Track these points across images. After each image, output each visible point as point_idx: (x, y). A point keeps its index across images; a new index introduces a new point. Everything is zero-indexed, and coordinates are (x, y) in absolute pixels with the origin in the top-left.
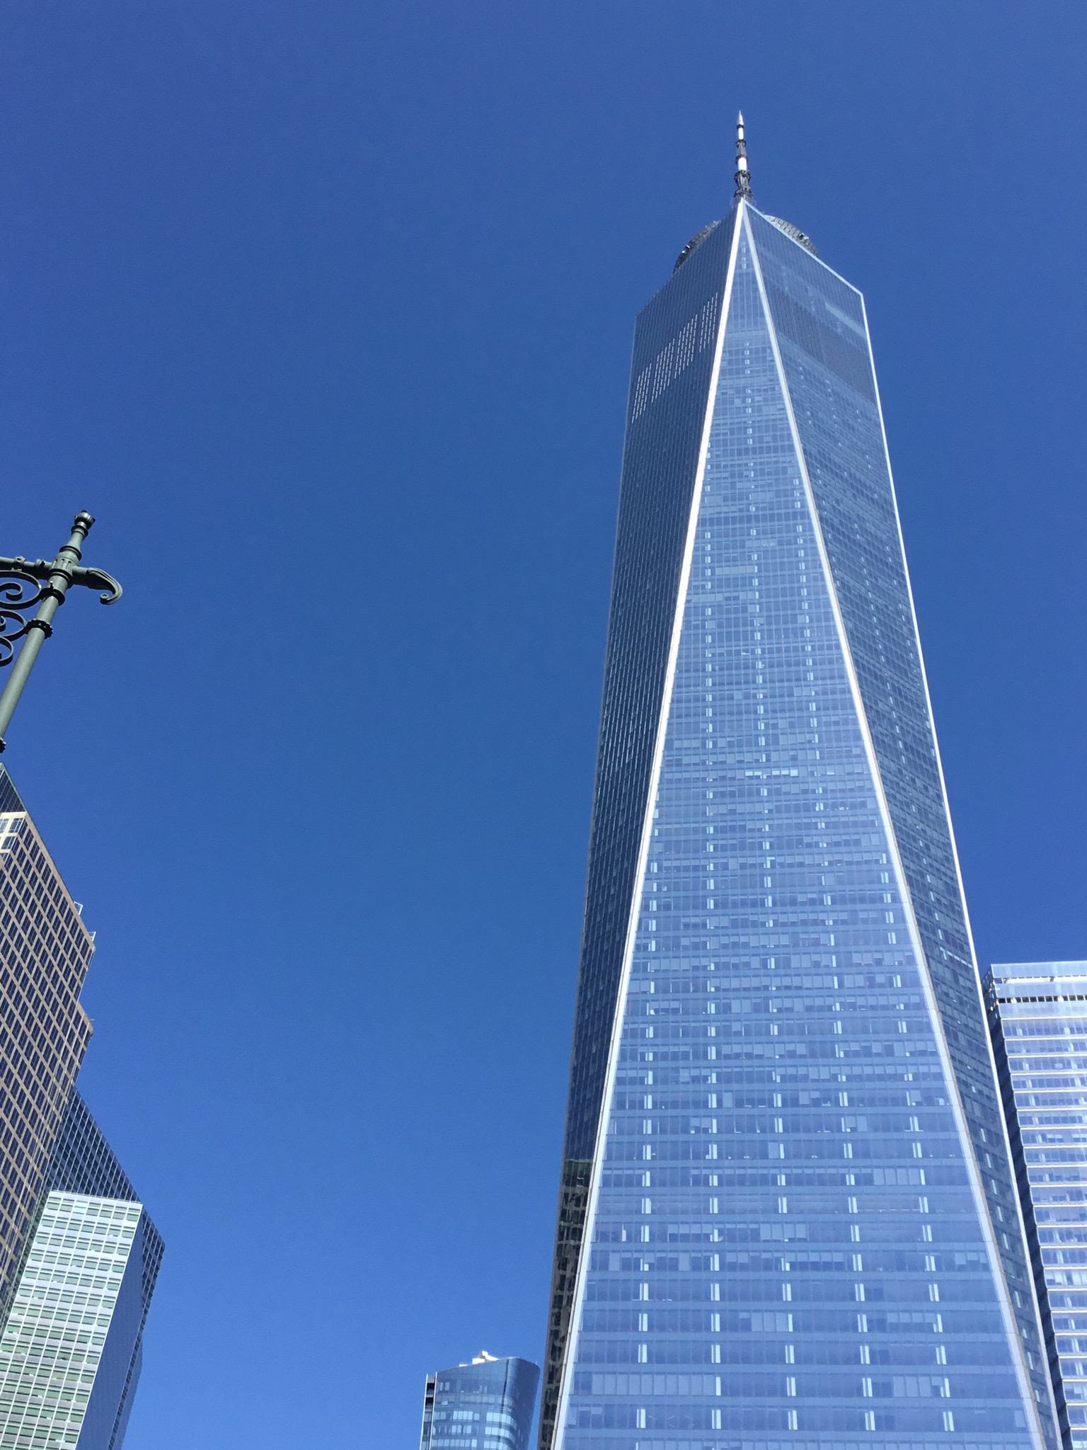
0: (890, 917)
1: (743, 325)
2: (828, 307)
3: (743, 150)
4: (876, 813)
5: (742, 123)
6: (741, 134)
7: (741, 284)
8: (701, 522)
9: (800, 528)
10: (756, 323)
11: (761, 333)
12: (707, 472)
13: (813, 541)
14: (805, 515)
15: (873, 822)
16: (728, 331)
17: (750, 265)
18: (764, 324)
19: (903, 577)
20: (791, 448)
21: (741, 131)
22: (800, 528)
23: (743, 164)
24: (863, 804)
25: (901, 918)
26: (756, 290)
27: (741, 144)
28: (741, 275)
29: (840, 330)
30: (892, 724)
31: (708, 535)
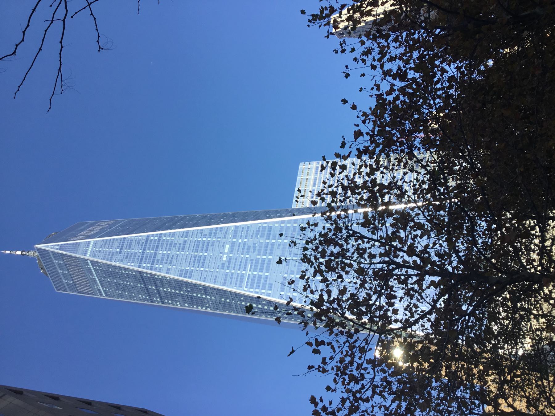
0: (277, 225)
2: (80, 229)
3: (12, 252)
6: (8, 252)
8: (139, 266)
9: (152, 238)
13: (157, 234)
14: (148, 236)
18: (80, 243)
20: (124, 238)
22: (152, 238)
23: (19, 253)
25: (277, 222)
26: (67, 244)
27: (12, 252)
31: (144, 265)
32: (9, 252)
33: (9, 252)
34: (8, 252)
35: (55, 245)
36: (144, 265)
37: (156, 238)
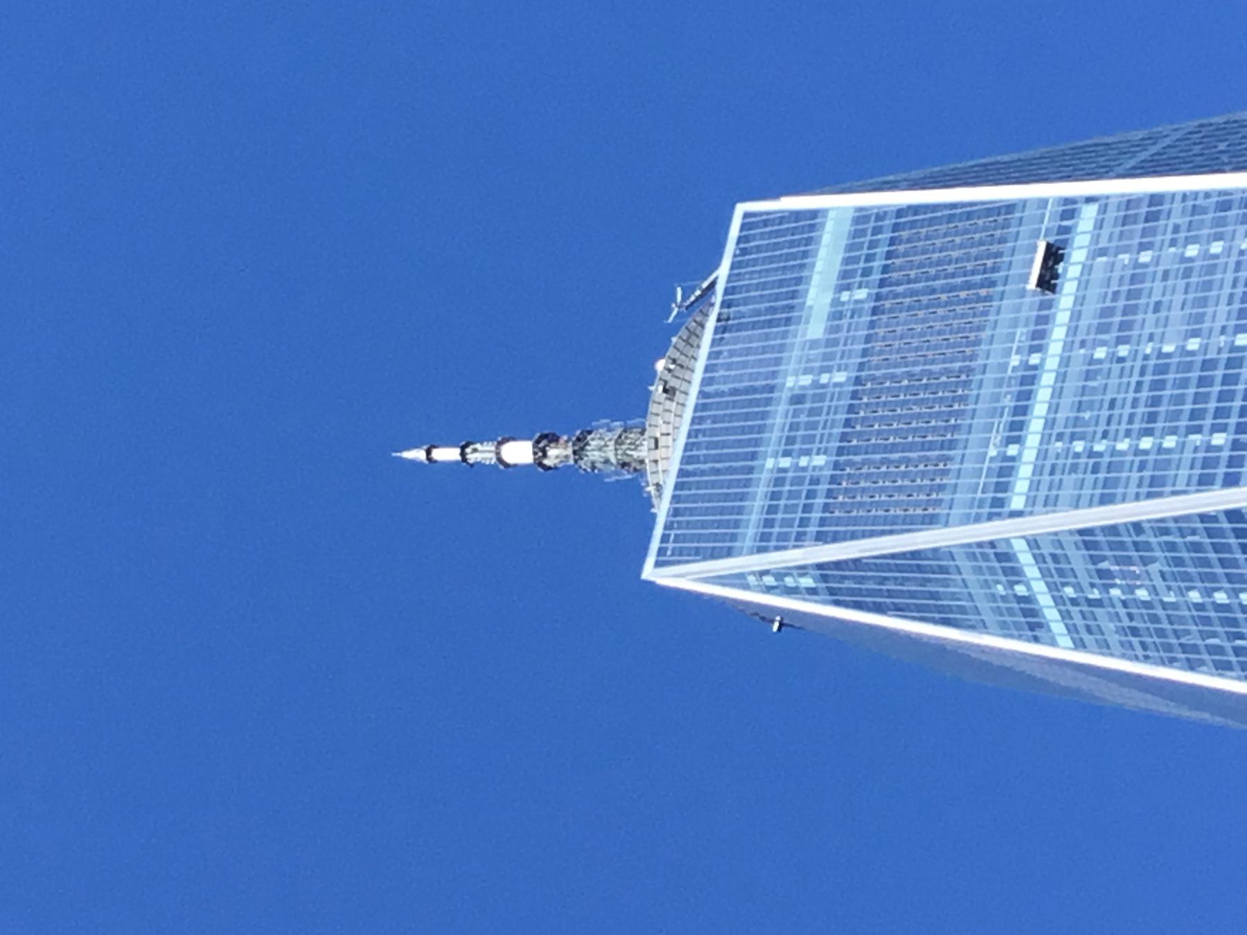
1: (954, 597)
2: (815, 329)
3: (482, 453)
5: (419, 454)
6: (447, 454)
7: (852, 592)
10: (943, 570)
11: (964, 564)
16: (982, 627)
17: (802, 570)
21: (438, 454)
23: (519, 452)
26: (856, 562)
27: (472, 458)
28: (832, 591)
29: (861, 294)
34: (447, 454)
35: (780, 575)
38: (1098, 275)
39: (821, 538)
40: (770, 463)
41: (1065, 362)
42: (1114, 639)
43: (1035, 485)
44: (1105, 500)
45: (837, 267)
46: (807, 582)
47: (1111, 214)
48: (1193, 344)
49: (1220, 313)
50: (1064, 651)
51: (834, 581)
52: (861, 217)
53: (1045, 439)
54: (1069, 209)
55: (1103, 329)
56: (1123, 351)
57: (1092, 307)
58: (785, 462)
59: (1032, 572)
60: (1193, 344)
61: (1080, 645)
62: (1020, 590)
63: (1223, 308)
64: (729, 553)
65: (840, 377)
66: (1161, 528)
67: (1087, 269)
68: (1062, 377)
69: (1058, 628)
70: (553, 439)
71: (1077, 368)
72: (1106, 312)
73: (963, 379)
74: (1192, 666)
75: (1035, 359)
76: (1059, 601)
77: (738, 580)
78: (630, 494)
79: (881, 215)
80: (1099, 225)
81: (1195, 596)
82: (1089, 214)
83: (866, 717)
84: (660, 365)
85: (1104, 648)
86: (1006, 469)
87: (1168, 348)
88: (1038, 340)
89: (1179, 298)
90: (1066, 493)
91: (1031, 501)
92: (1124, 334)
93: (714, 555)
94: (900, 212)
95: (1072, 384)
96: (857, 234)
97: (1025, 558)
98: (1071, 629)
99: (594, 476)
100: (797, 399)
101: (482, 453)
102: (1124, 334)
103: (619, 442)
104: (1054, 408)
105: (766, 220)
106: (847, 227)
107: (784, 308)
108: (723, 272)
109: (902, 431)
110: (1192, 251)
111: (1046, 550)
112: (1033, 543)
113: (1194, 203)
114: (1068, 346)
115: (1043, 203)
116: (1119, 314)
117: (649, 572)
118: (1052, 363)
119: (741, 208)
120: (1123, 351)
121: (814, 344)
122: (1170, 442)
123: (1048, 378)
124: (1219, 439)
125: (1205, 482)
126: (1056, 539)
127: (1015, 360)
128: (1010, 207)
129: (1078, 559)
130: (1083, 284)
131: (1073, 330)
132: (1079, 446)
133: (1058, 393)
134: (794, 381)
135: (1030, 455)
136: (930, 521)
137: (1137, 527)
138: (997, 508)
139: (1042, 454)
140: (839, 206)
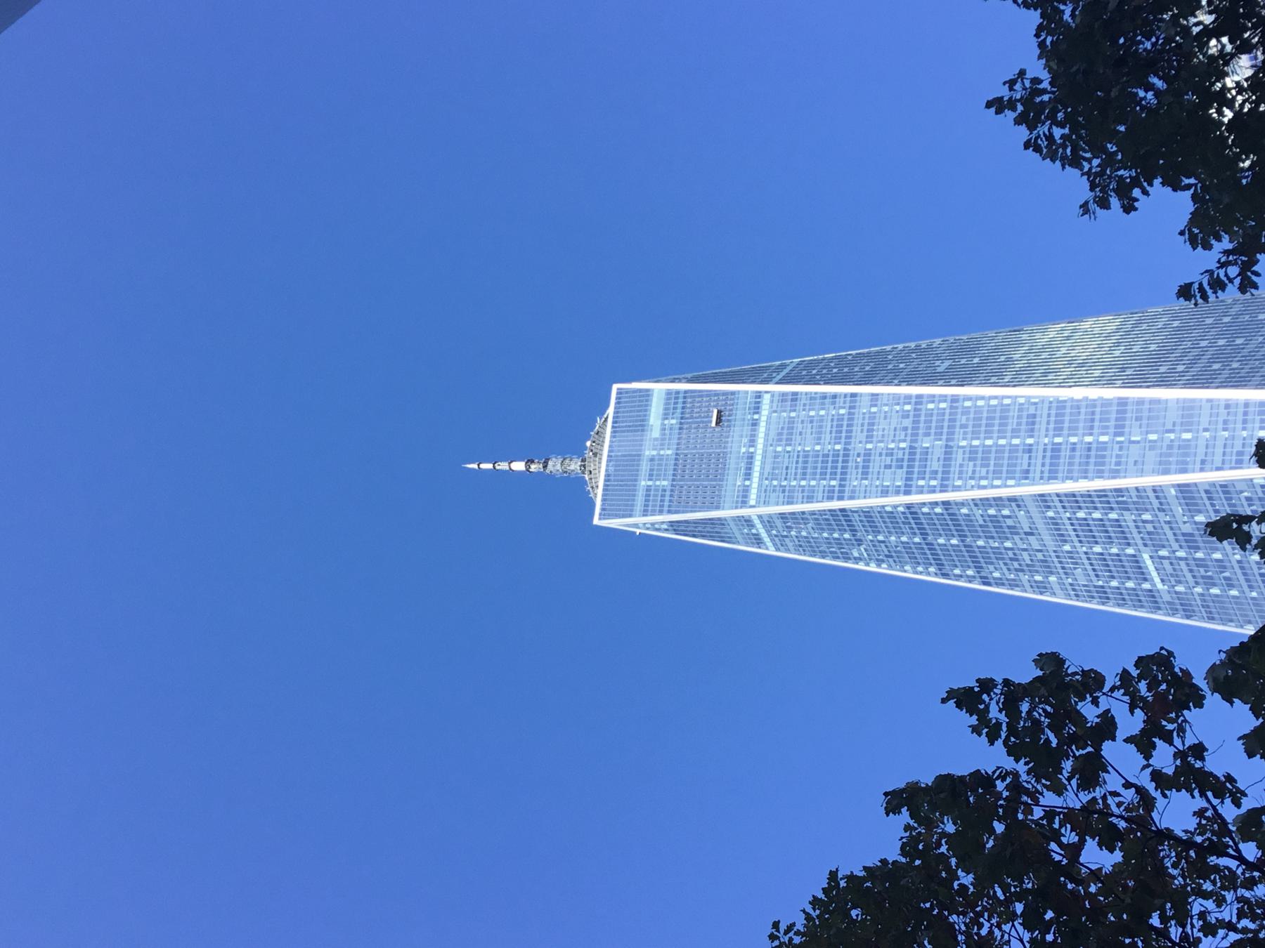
2: (656, 433)
3: (503, 466)
4: (1213, 484)
5: (475, 466)
6: (487, 466)
8: (945, 575)
12: (890, 567)
14: (909, 506)
15: (1221, 486)
16: (738, 543)
18: (719, 519)
19: (919, 396)
20: (842, 510)
21: (482, 466)
22: (925, 510)
23: (519, 466)
24: (1207, 492)
26: (686, 522)
30: (1103, 447)
32: (490, 466)
33: (490, 466)
34: (487, 466)
35: (653, 524)
36: (957, 571)
37: (938, 510)
38: (774, 420)
39: (669, 512)
40: (643, 483)
41: (765, 451)
42: (792, 549)
43: (759, 497)
44: (788, 503)
45: (661, 411)
46: (665, 526)
47: (776, 399)
48: (818, 448)
49: (827, 437)
50: (772, 552)
51: (675, 526)
52: (669, 393)
53: (761, 479)
54: (759, 395)
55: (780, 440)
56: (789, 448)
57: (773, 434)
58: (650, 483)
59: (759, 526)
60: (818, 448)
61: (778, 549)
62: (754, 531)
63: (828, 436)
64: (630, 516)
65: (669, 452)
66: (813, 513)
67: (769, 417)
68: (764, 457)
69: (769, 544)
70: (532, 462)
71: (770, 455)
72: (780, 434)
73: (721, 459)
74: (823, 557)
75: (752, 450)
76: (770, 535)
77: (636, 526)
78: (576, 489)
79: (678, 392)
80: (772, 401)
81: (825, 535)
82: (767, 397)
83: (698, 576)
84: (588, 444)
85: (788, 551)
86: (746, 491)
87: (807, 449)
88: (752, 442)
89: (809, 431)
90: (773, 499)
91: (758, 502)
92: (789, 442)
93: (624, 516)
94: (686, 392)
95: (769, 460)
96: (668, 399)
97: (757, 522)
98: (775, 545)
99: (551, 475)
100: (652, 460)
101: (503, 466)
102: (789, 442)
103: (562, 464)
104: (762, 468)
105: (627, 391)
106: (663, 396)
107: (641, 425)
108: (611, 411)
109: (699, 474)
110: (812, 413)
111: (766, 519)
112: (760, 517)
113: (812, 397)
114: (765, 446)
115: (747, 392)
116: (786, 433)
117: (596, 521)
118: (760, 452)
119: (615, 387)
120: (789, 448)
121: (656, 439)
122: (813, 483)
123: (758, 458)
124: (833, 483)
125: (830, 498)
126: (770, 516)
127: (743, 450)
128: (733, 393)
129: (779, 523)
130: (768, 423)
131: (766, 440)
132: (775, 483)
133: (763, 463)
134: (649, 453)
135: (755, 485)
136: (718, 508)
137: (803, 513)
138: (744, 503)
139: (760, 485)
140: (659, 388)
